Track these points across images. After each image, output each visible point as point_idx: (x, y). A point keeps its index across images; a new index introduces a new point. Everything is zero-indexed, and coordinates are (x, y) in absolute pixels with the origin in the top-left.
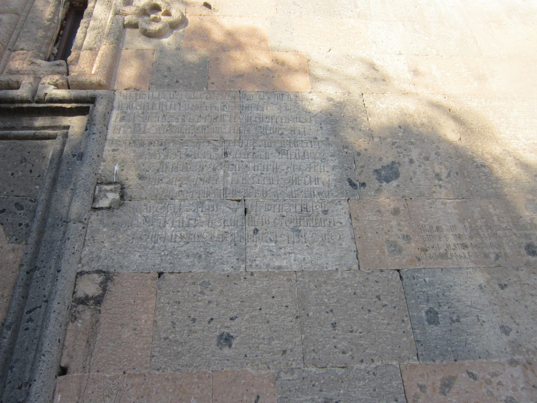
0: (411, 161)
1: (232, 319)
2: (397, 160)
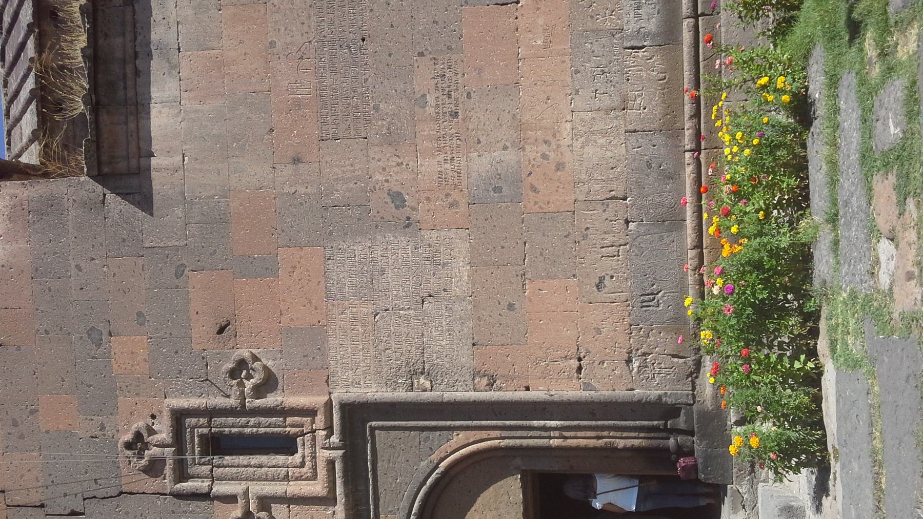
0: (387, 181)
1: (499, 304)
2: (387, 192)
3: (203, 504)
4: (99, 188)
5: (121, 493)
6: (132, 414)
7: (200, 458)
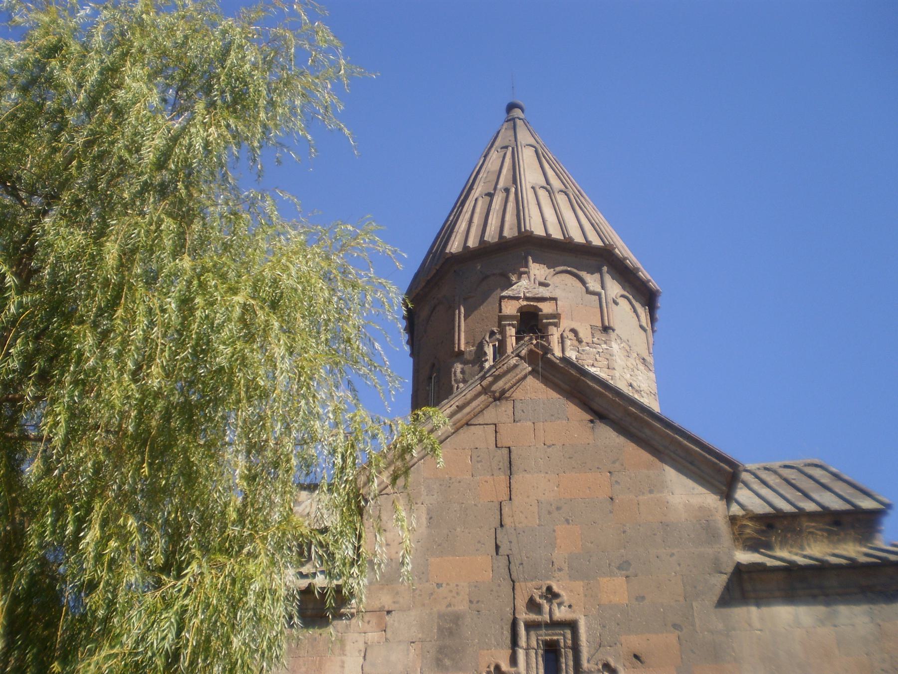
3: (508, 641)
4: (730, 569)
5: (513, 581)
6: (571, 591)
7: (542, 641)
